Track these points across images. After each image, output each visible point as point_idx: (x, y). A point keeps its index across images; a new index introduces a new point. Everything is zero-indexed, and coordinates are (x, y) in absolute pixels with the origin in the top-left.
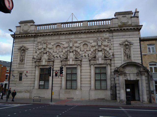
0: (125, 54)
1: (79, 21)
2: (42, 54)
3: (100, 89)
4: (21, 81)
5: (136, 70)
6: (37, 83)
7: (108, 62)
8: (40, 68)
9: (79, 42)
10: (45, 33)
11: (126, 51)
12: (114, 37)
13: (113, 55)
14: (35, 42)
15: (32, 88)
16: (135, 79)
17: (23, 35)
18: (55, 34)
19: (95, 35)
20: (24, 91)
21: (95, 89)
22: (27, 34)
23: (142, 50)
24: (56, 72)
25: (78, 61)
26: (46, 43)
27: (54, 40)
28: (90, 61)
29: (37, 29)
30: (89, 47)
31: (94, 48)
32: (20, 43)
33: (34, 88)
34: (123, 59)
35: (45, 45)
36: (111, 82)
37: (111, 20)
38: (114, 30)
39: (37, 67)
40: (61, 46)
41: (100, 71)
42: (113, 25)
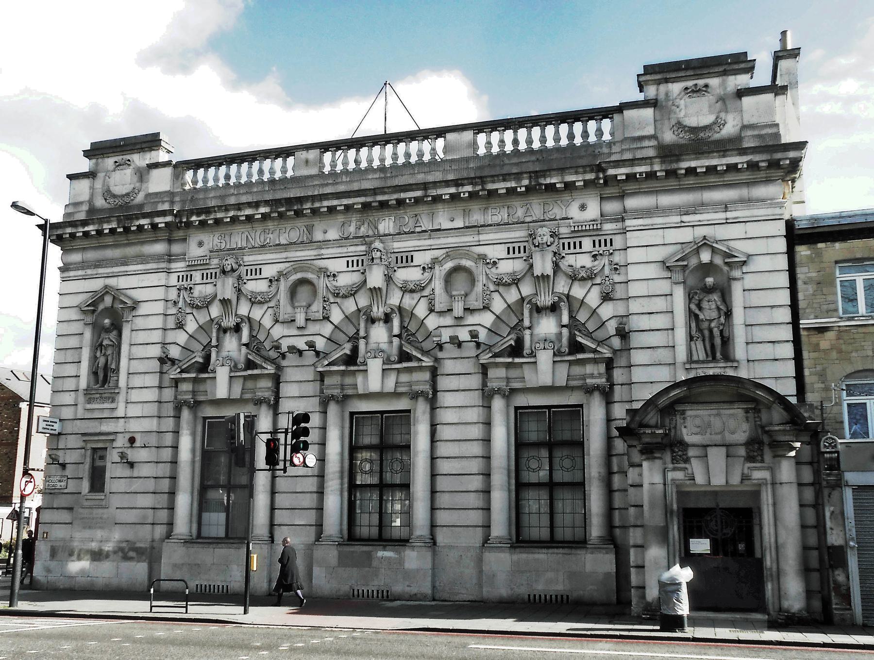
0: (693, 325)
1: (423, 126)
2: (214, 335)
4: (100, 496)
5: (745, 426)
11: (705, 305)
12: (628, 223)
14: (174, 265)
17: (107, 227)
21: (518, 541)
23: (801, 296)
25: (414, 374)
26: (233, 270)
28: (484, 369)
29: (183, 184)
30: (479, 288)
32: (89, 272)
33: (169, 535)
34: (681, 354)
35: (230, 281)
39: (186, 414)
40: (322, 283)
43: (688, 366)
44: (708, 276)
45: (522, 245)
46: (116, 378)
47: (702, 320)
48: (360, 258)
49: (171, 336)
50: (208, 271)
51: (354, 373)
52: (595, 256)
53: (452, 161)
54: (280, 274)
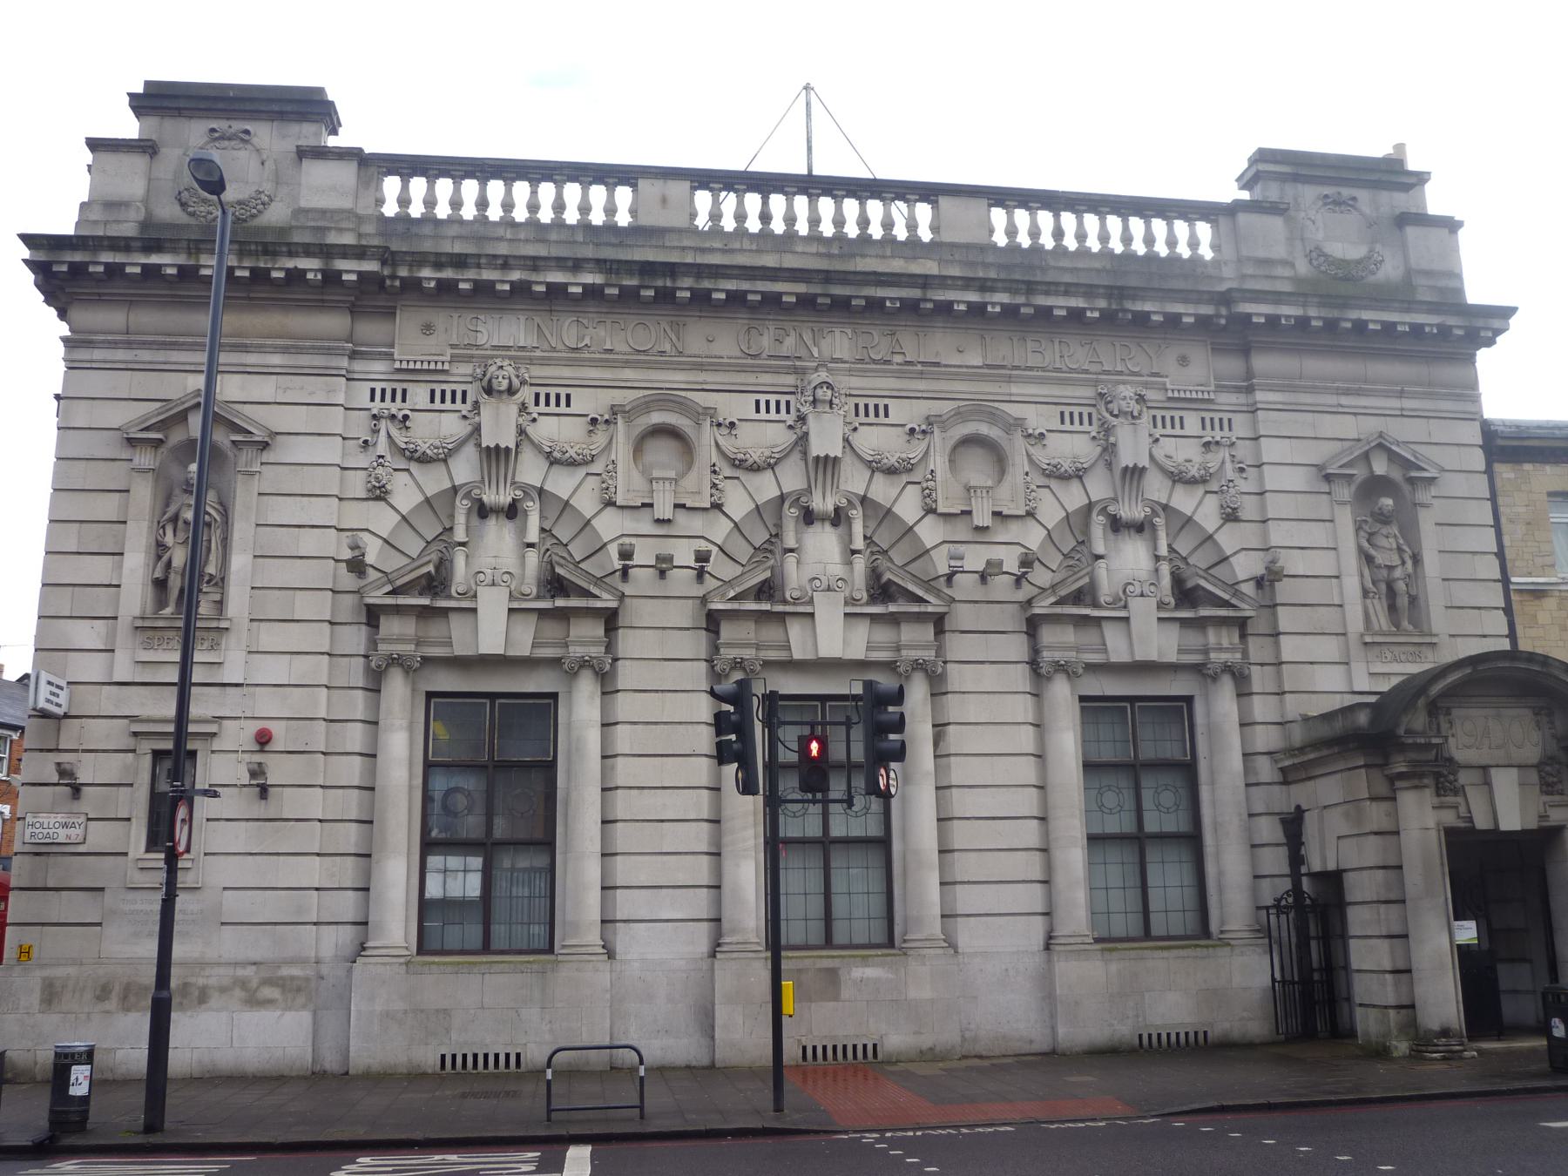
0: (1366, 572)
1: (883, 174)
2: (461, 518)
3: (1140, 932)
5: (1536, 736)
6: (396, 873)
7: (1222, 646)
8: (430, 695)
9: (901, 412)
10: (506, 263)
12: (1260, 396)
13: (1267, 581)
14: (359, 366)
15: (334, 941)
16: (1533, 824)
18: (629, 297)
19: (1076, 353)
20: (223, 990)
22: (270, 250)
23: (1506, 541)
24: (814, 746)
26: (511, 391)
27: (608, 359)
28: (1033, 626)
29: (380, 202)
31: (1075, 486)
34: (1355, 624)
35: (510, 410)
36: (1254, 862)
37: (1222, 219)
38: (1273, 320)
40: (706, 439)
41: (1141, 745)
42: (1250, 271)
43: (1368, 639)
44: (1388, 496)
45: (1085, 411)
46: (217, 597)
47: (1379, 567)
48: (783, 399)
49: (357, 515)
50: (444, 386)
51: (781, 617)
52: (1207, 445)
53: (953, 245)
54: (615, 410)
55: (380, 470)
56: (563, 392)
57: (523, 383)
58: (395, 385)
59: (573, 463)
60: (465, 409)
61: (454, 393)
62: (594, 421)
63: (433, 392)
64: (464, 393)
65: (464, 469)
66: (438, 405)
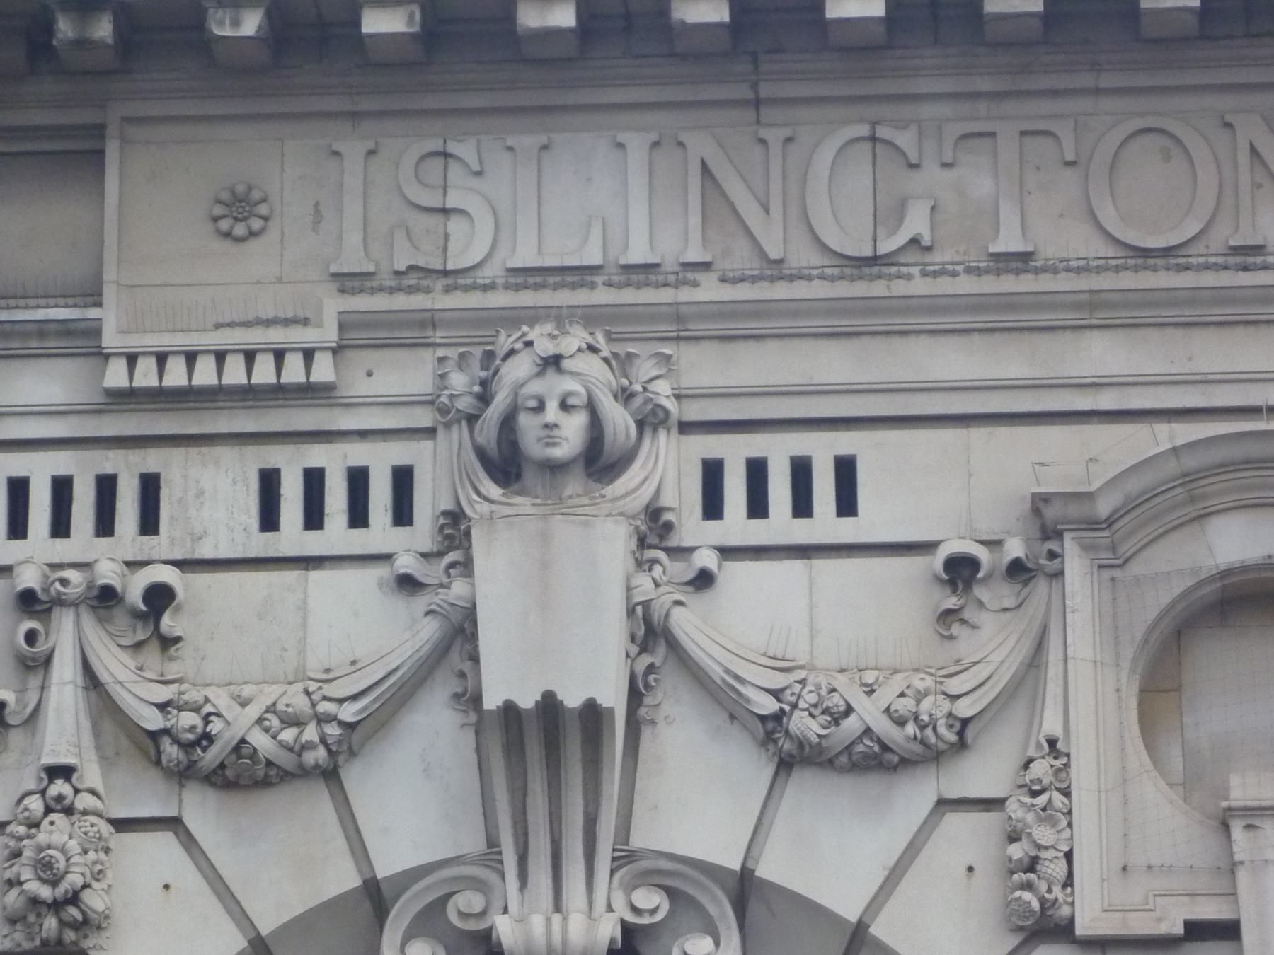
26: (599, 461)
35: (598, 545)
50: (317, 455)
54: (1049, 518)
55: (57, 831)
56: (823, 450)
57: (651, 420)
58: (110, 462)
59: (875, 760)
60: (408, 546)
61: (358, 480)
62: (960, 571)
63: (269, 482)
64: (403, 479)
65: (414, 807)
66: (291, 536)
